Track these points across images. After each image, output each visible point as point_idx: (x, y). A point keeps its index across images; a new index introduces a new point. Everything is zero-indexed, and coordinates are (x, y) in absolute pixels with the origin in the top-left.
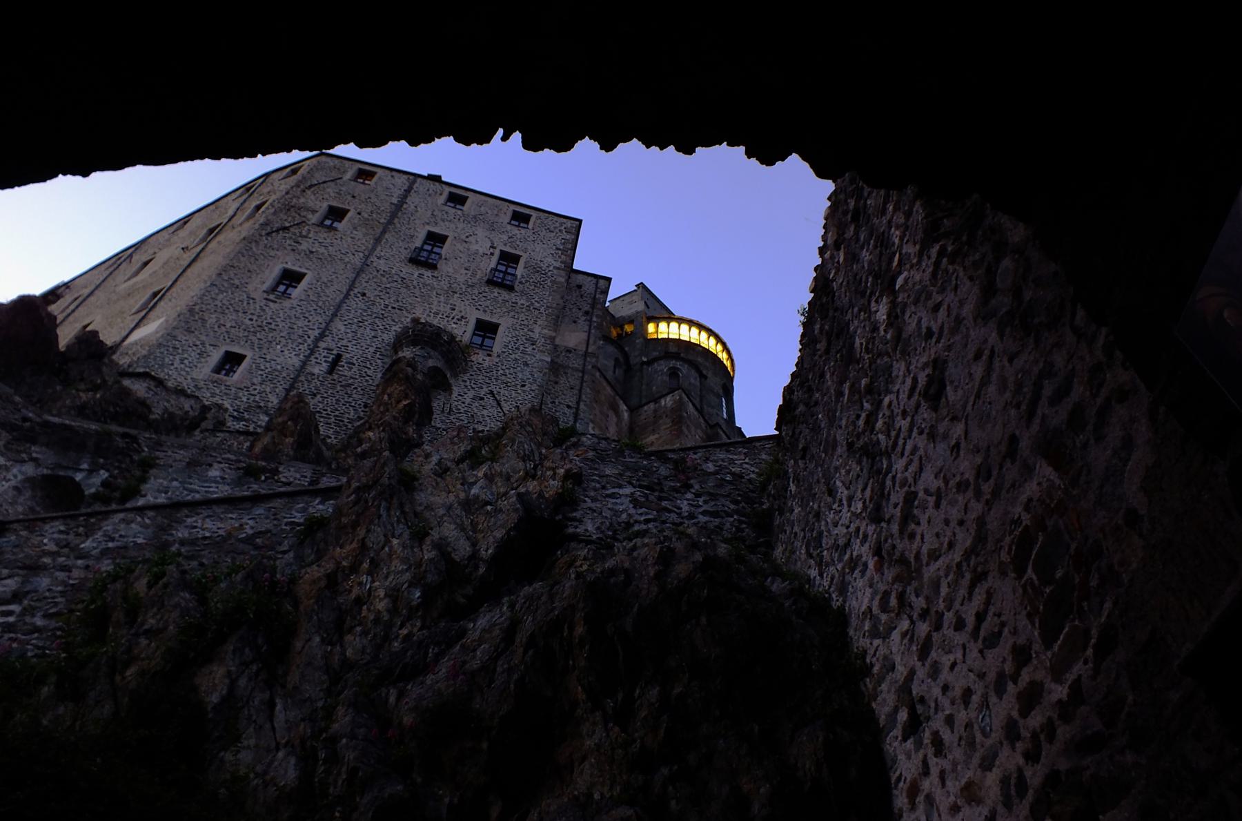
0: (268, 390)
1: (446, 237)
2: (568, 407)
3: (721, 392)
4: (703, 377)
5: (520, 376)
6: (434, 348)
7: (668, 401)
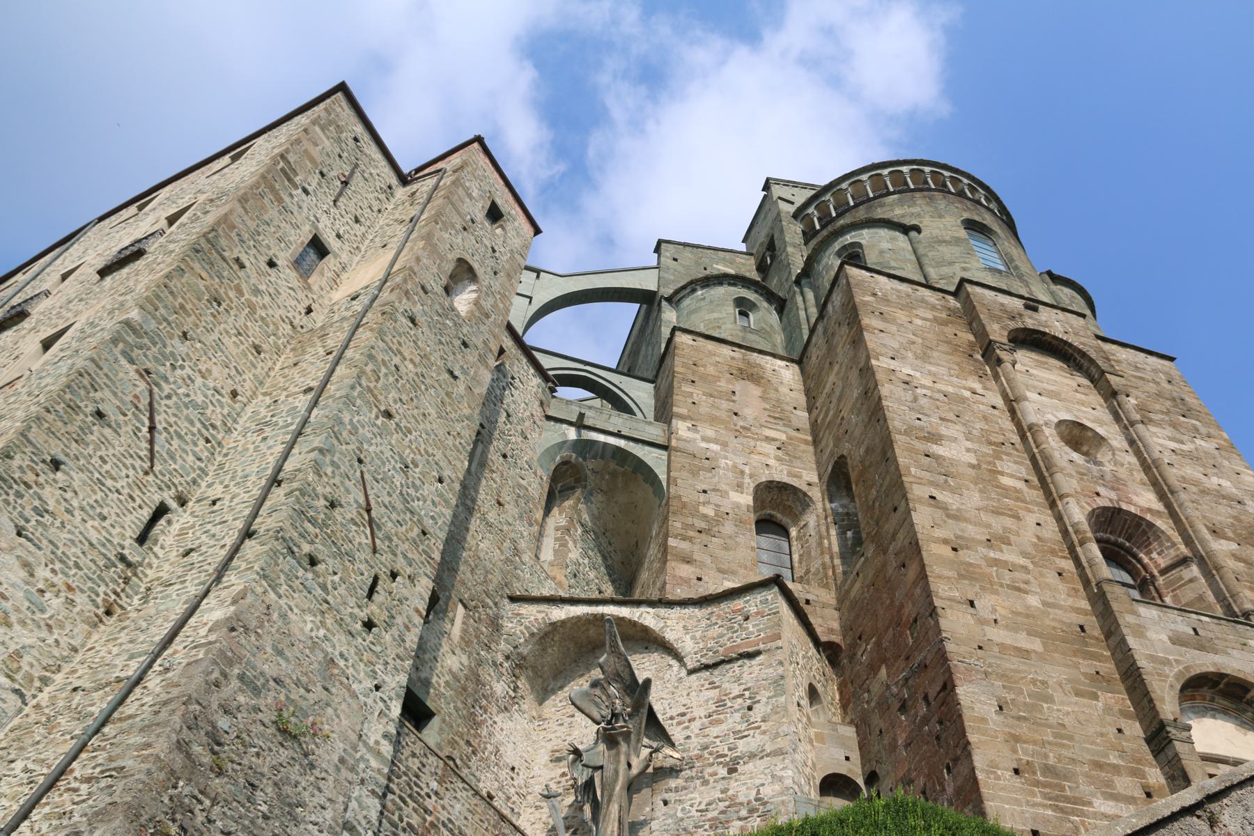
3: (963, 233)
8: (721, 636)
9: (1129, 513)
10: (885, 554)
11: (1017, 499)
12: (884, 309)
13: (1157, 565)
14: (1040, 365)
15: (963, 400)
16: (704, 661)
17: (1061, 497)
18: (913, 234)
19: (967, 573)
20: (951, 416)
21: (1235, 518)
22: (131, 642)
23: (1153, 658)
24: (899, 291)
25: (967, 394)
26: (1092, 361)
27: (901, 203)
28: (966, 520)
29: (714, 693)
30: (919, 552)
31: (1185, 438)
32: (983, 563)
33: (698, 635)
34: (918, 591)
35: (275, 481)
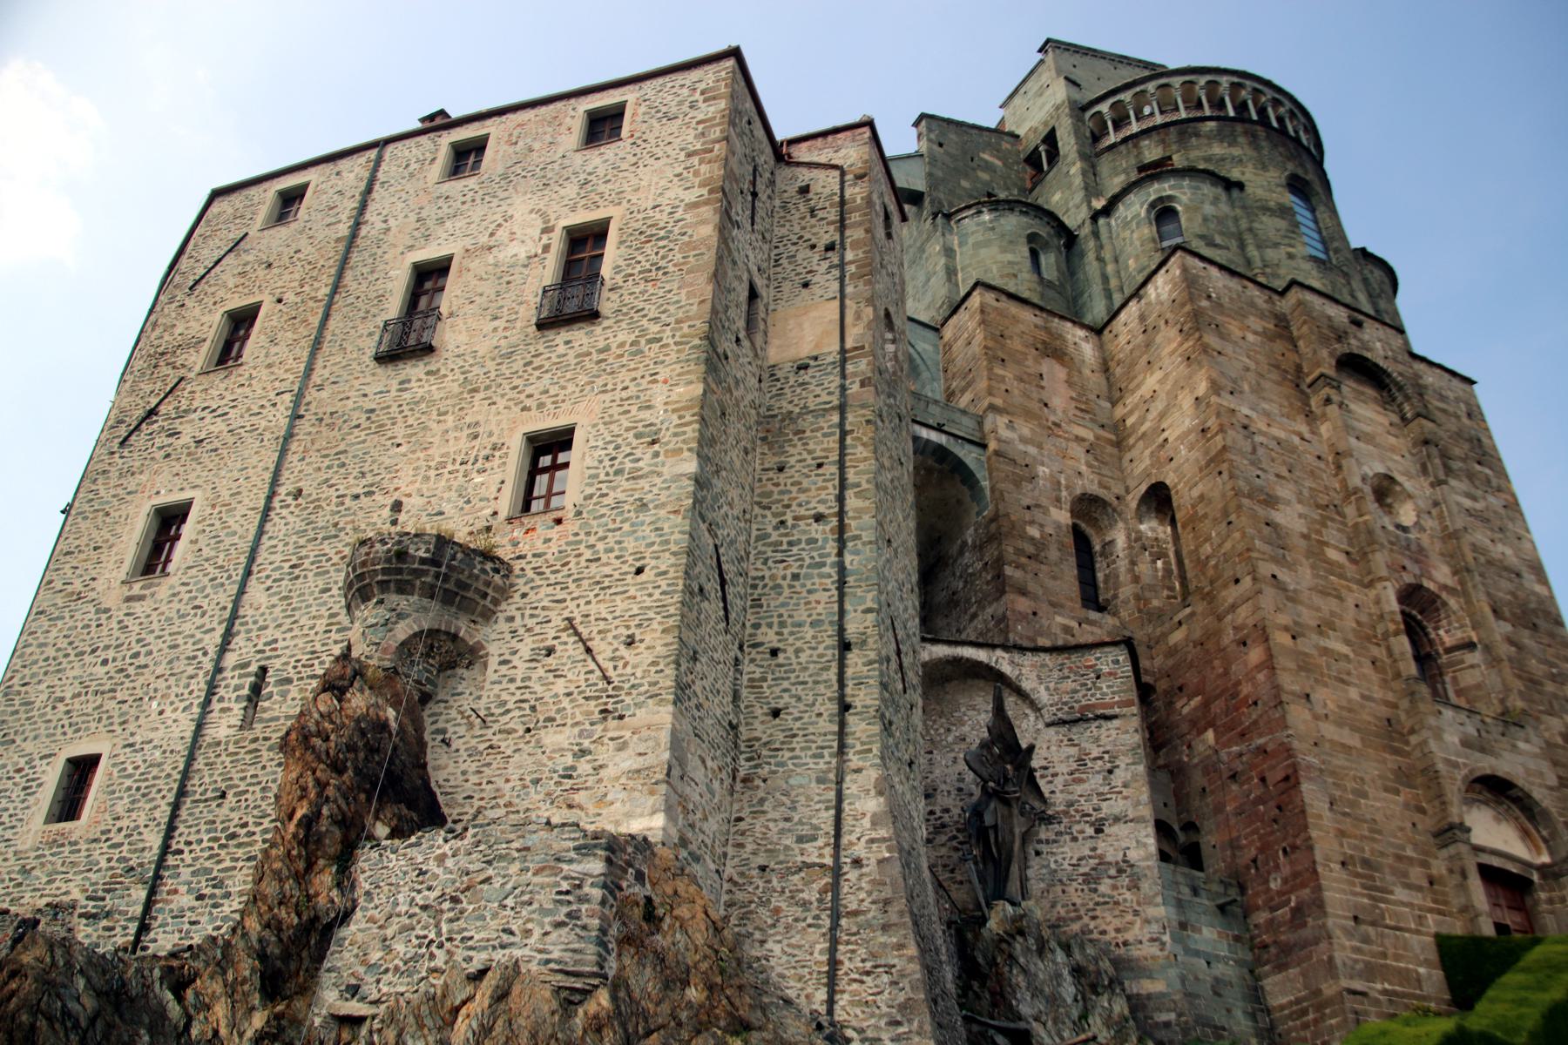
0: (142, 822)
1: (449, 259)
2: (819, 518)
4: (1231, 185)
5: (630, 544)
6: (402, 588)
7: (1161, 289)
8: (1076, 692)
9: (1428, 590)
10: (1220, 618)
11: (1341, 576)
12: (1220, 318)
13: (1443, 643)
14: (1359, 397)
15: (1293, 450)
16: (1060, 715)
17: (1381, 579)
18: (1235, 193)
19: (1305, 666)
20: (1285, 473)
21: (1513, 594)
22: (787, 820)
23: (1448, 762)
24: (1230, 290)
25: (1296, 440)
26: (1407, 398)
27: (1220, 136)
28: (1301, 603)
29: (1073, 751)
30: (1267, 640)
31: (1479, 493)
32: (1314, 652)
33: (1052, 685)
34: (1261, 677)
35: (845, 646)
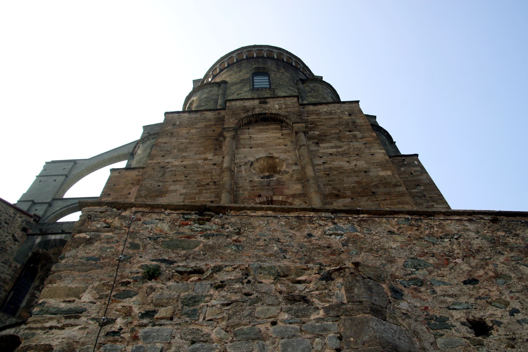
18: (222, 85)
